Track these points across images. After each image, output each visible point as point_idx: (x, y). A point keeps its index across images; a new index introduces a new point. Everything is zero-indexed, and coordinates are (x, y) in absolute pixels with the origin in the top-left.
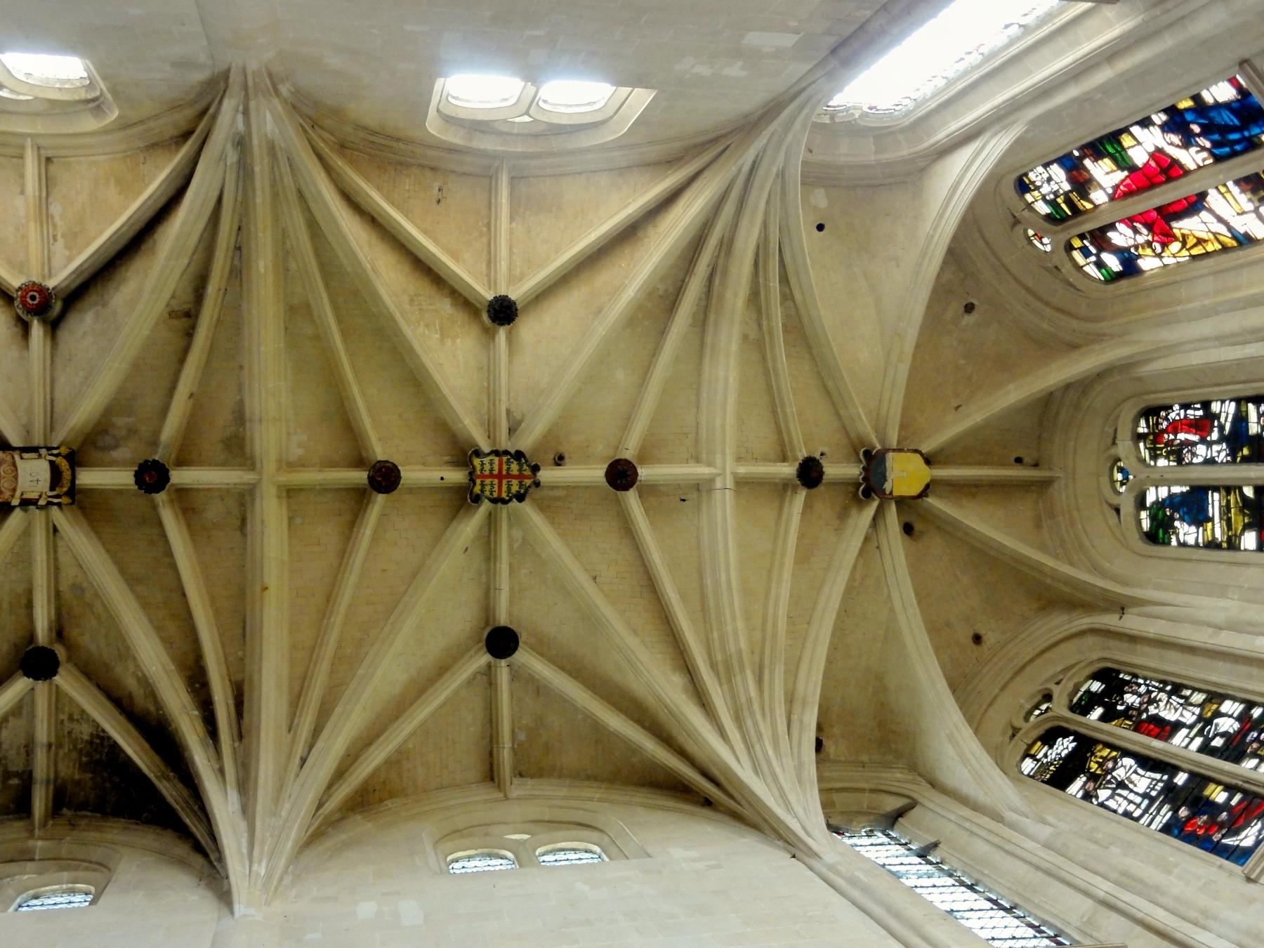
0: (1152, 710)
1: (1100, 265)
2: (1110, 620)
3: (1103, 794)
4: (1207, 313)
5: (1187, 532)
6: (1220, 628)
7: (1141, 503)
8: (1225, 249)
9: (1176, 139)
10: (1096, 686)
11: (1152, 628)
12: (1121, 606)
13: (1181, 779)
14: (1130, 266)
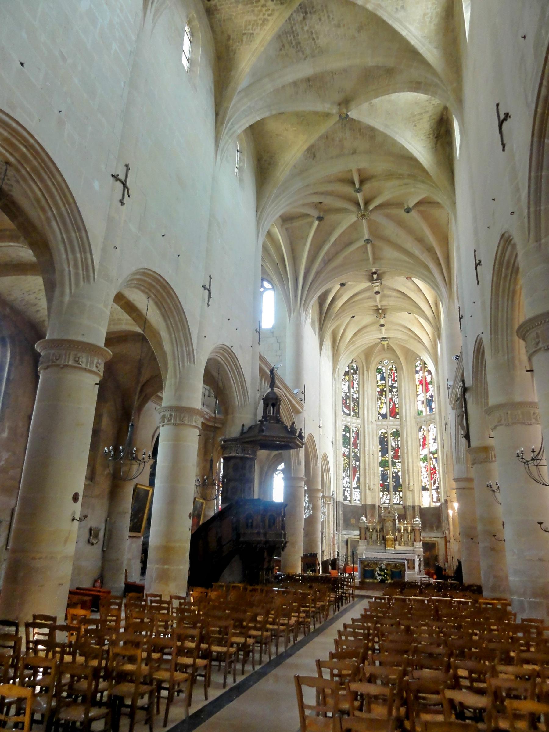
0: (354, 382)
1: (418, 366)
2: (365, 369)
3: (343, 383)
4: (409, 387)
5: (379, 376)
6: (367, 391)
7: (382, 367)
8: (417, 392)
9: (430, 394)
10: (355, 368)
11: (365, 379)
12: (368, 371)
13: (348, 394)
14: (417, 372)
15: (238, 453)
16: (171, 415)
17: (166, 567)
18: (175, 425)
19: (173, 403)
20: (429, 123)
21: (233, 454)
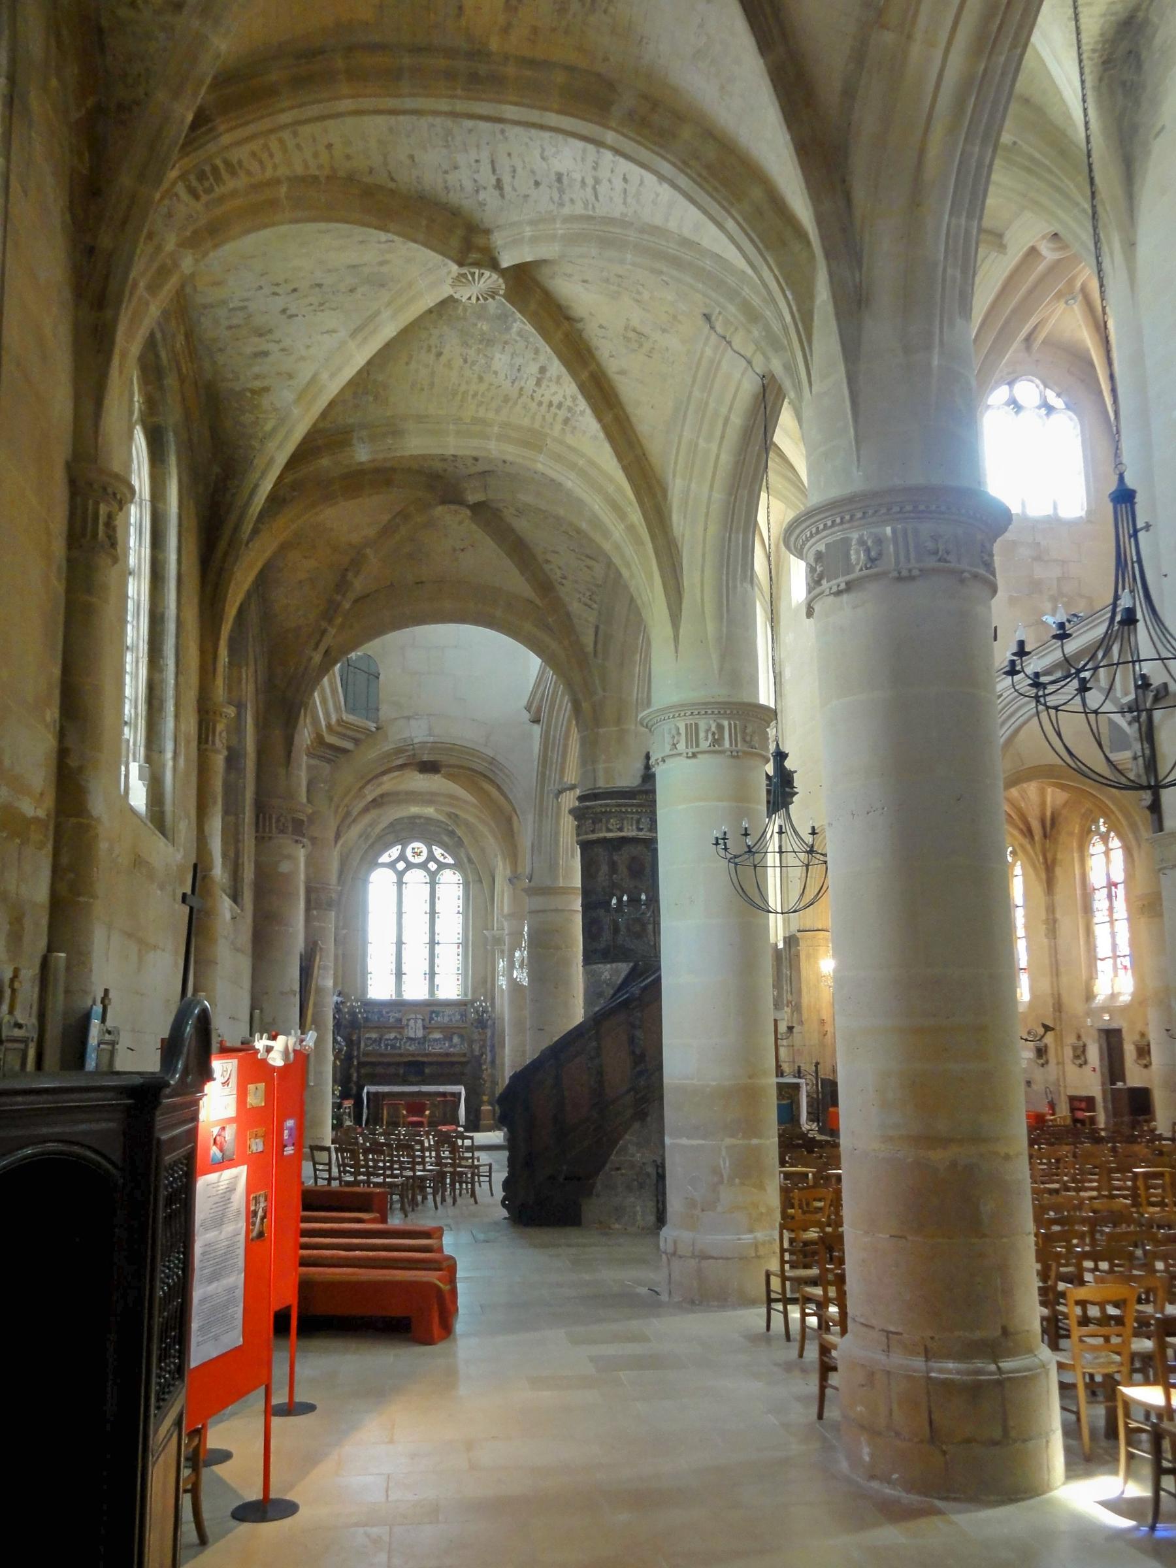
15: (641, 830)
16: (720, 727)
17: (755, 1141)
18: (735, 756)
19: (720, 693)
20: (1102, 20)
21: (630, 832)
